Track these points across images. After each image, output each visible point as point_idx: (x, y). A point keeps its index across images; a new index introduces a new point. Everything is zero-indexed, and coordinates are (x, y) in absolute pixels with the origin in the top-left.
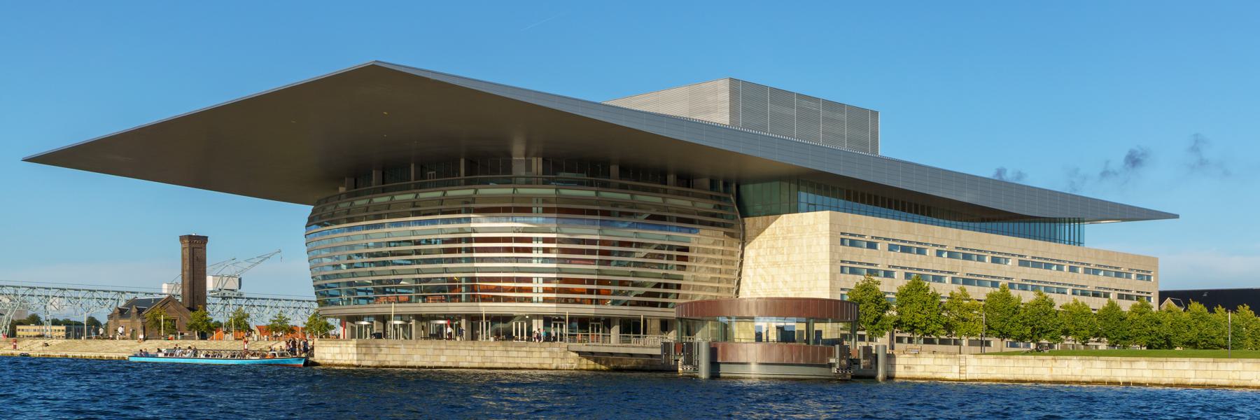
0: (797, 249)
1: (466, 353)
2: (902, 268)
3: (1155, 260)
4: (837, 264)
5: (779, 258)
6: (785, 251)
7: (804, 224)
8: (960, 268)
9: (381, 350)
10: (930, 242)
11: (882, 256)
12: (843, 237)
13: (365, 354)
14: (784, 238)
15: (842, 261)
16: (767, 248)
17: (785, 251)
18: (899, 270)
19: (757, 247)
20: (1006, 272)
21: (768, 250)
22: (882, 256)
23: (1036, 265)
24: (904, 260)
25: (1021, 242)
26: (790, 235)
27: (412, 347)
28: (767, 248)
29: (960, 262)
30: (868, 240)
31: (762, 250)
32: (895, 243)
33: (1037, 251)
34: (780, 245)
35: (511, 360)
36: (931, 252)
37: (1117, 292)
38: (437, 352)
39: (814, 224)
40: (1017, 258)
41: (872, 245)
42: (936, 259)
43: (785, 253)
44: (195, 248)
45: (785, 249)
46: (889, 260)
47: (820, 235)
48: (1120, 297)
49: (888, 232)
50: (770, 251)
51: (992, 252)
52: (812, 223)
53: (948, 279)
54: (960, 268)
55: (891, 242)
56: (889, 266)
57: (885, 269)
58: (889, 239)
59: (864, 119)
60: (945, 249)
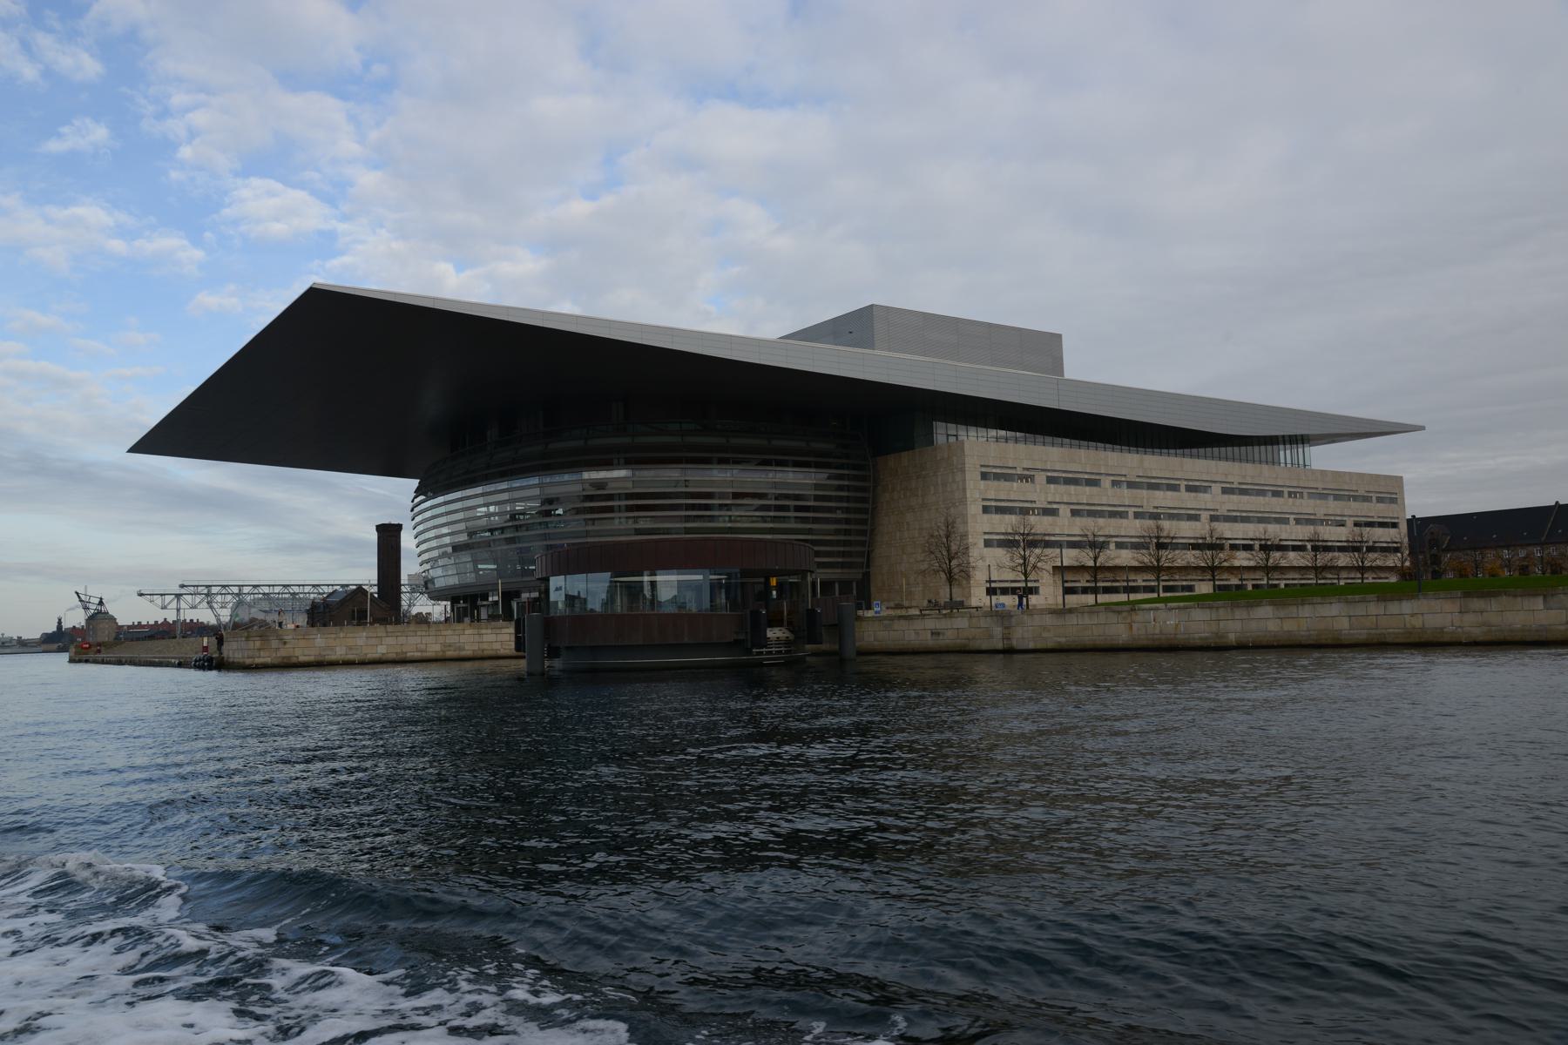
0: (932, 488)
1: (418, 640)
3: (1399, 480)
6: (920, 493)
8: (1145, 504)
9: (285, 643)
12: (984, 470)
13: (259, 650)
15: (984, 499)
18: (1066, 506)
25: (1223, 466)
27: (333, 636)
29: (1145, 492)
32: (1055, 474)
33: (1244, 477)
35: (485, 646)
38: (373, 641)
41: (1027, 478)
42: (1110, 491)
44: (389, 536)
49: (1046, 461)
51: (1186, 480)
55: (1049, 474)
56: (1050, 503)
58: (1049, 471)
59: (1051, 343)
60: (1123, 479)
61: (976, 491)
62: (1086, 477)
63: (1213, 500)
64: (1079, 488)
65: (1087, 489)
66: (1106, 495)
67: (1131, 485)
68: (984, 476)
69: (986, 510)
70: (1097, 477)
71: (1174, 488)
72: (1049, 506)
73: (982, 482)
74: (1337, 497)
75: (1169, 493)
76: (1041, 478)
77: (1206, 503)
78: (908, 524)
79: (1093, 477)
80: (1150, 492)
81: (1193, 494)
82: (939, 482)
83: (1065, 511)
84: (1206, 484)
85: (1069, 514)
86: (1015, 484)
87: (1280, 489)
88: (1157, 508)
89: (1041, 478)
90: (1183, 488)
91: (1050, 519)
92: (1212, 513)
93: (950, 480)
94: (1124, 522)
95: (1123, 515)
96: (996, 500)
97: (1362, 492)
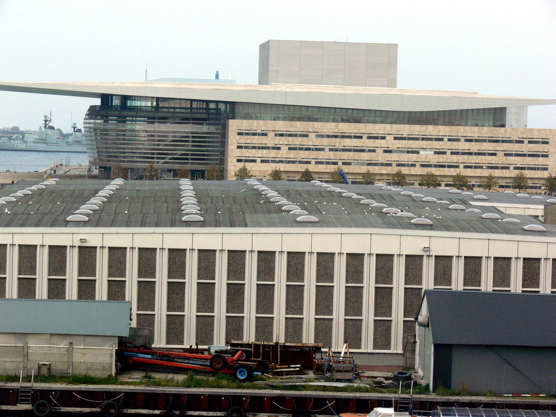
2: (285, 145)
4: (234, 144)
10: (310, 131)
11: (269, 139)
12: (239, 131)
20: (381, 144)
22: (269, 139)
23: (409, 139)
24: (289, 141)
29: (337, 140)
30: (259, 132)
33: (413, 132)
36: (313, 136)
37: (503, 152)
40: (392, 137)
46: (276, 141)
48: (506, 155)
53: (327, 149)
54: (337, 143)
56: (275, 144)
57: (272, 146)
61: (233, 140)
62: (300, 133)
63: (390, 143)
64: (294, 138)
65: (300, 138)
66: (312, 141)
67: (329, 136)
68: (239, 134)
69: (239, 147)
70: (307, 133)
71: (361, 137)
72: (276, 146)
73: (238, 136)
74: (490, 141)
75: (355, 140)
76: (271, 135)
77: (381, 144)
79: (304, 133)
80: (342, 140)
81: (373, 140)
83: (284, 149)
84: (383, 135)
85: (287, 148)
86: (256, 137)
87: (440, 137)
88: (343, 146)
89: (271, 135)
90: (365, 137)
91: (276, 151)
92: (385, 149)
94: (322, 153)
95: (323, 150)
96: (245, 143)
97: (514, 138)
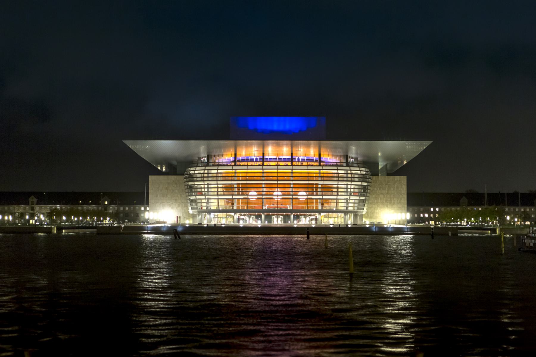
0: (392, 189)
5: (384, 192)
7: (395, 180)
14: (386, 185)
16: (378, 187)
17: (387, 190)
19: (373, 187)
21: (379, 188)
26: (388, 184)
28: (378, 187)
31: (375, 188)
34: (384, 187)
39: (400, 180)
43: (387, 190)
45: (386, 189)
47: (402, 184)
50: (379, 189)
52: (399, 180)
78: (381, 198)
82: (395, 187)
93: (400, 187)
